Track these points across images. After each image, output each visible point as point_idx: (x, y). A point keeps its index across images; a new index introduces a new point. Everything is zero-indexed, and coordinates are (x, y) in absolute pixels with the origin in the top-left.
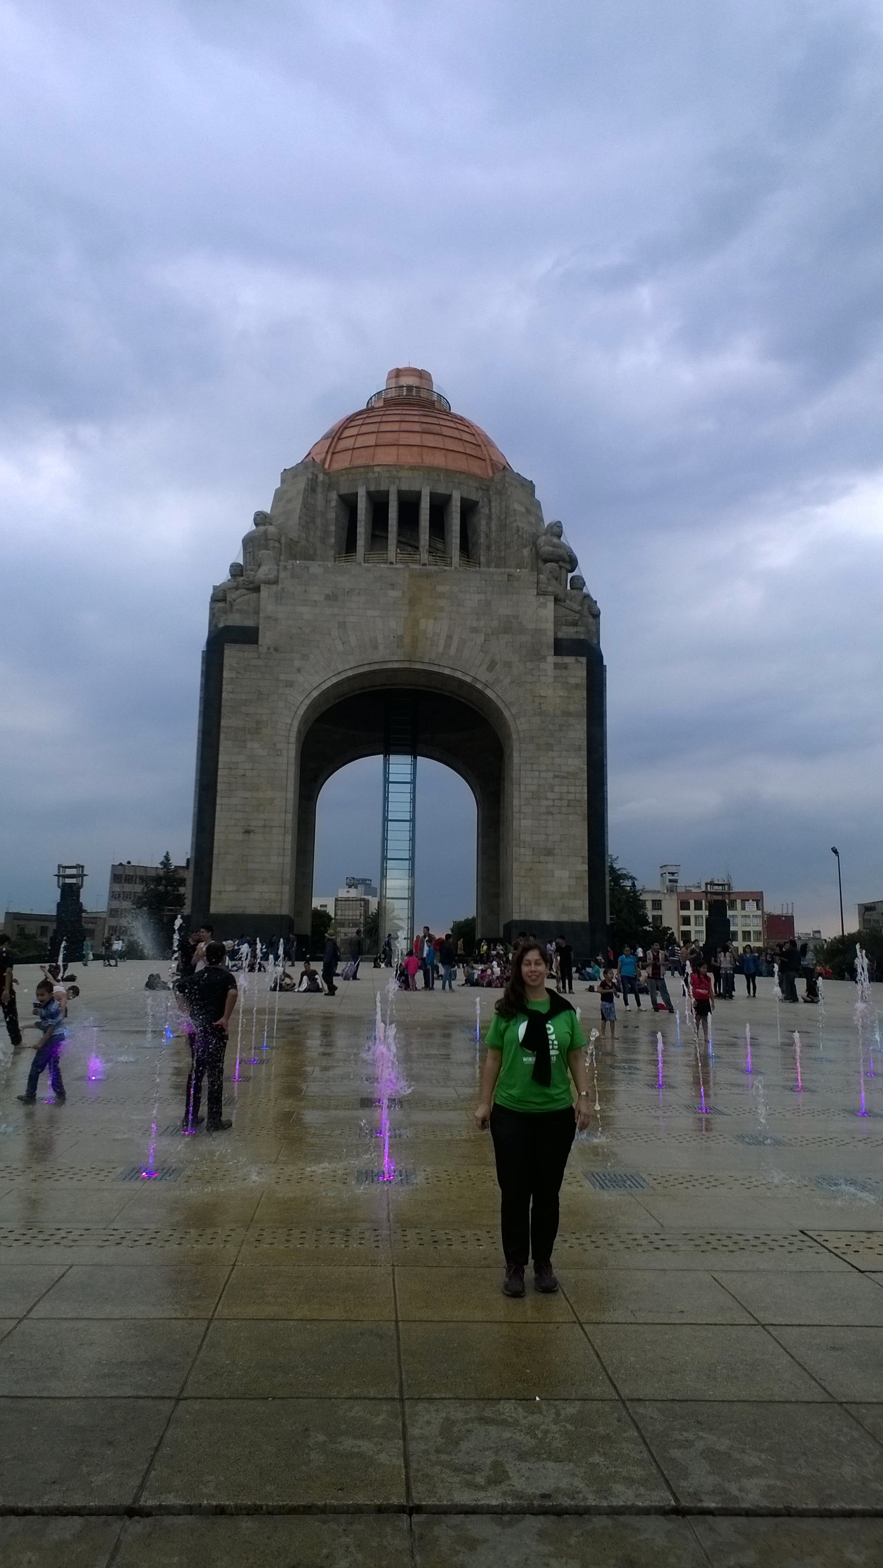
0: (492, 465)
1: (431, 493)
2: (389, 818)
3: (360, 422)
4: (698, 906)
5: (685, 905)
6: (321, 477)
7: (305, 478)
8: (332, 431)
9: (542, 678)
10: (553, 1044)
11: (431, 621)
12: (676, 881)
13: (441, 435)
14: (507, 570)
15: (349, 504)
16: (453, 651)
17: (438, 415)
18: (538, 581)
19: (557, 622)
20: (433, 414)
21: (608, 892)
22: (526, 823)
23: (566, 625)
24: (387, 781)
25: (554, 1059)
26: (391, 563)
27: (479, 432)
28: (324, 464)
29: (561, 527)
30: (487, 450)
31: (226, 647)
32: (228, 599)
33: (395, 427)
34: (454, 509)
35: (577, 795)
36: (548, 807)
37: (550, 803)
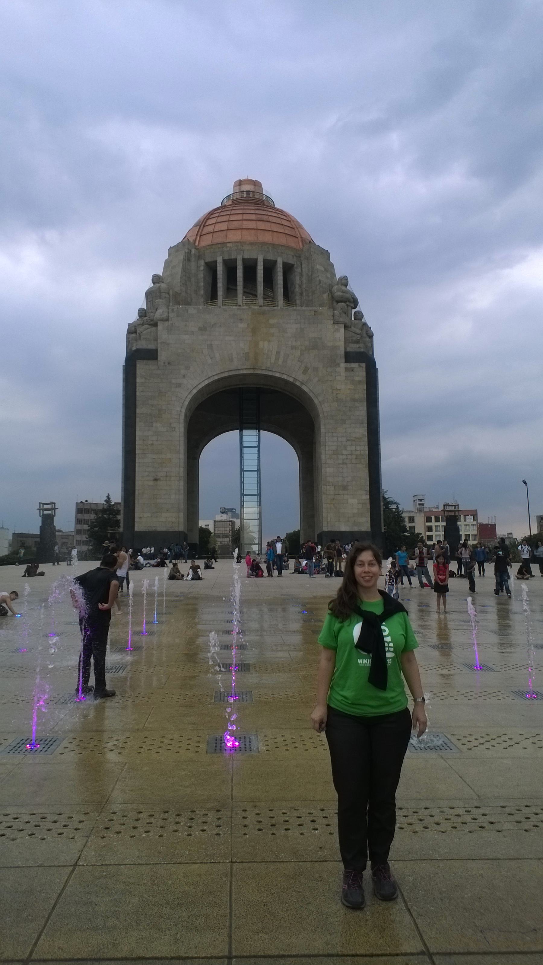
0: (302, 241)
1: (264, 260)
2: (244, 469)
3: (217, 215)
4: (437, 520)
5: (429, 520)
6: (193, 251)
7: (183, 252)
8: (199, 221)
9: (338, 378)
10: (389, 647)
11: (266, 343)
12: (423, 505)
13: (269, 222)
14: (313, 308)
15: (212, 267)
16: (280, 362)
17: (266, 209)
18: (333, 314)
19: (347, 341)
21: (382, 512)
22: (330, 470)
23: (352, 343)
24: (242, 446)
25: (389, 662)
26: (240, 306)
27: (293, 219)
28: (195, 243)
29: (347, 279)
30: (298, 231)
31: (137, 362)
32: (138, 332)
33: (240, 217)
34: (279, 269)
35: (362, 451)
36: (343, 459)
37: (345, 457)
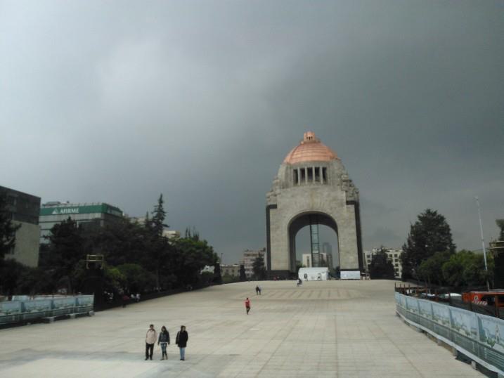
15: (296, 171)
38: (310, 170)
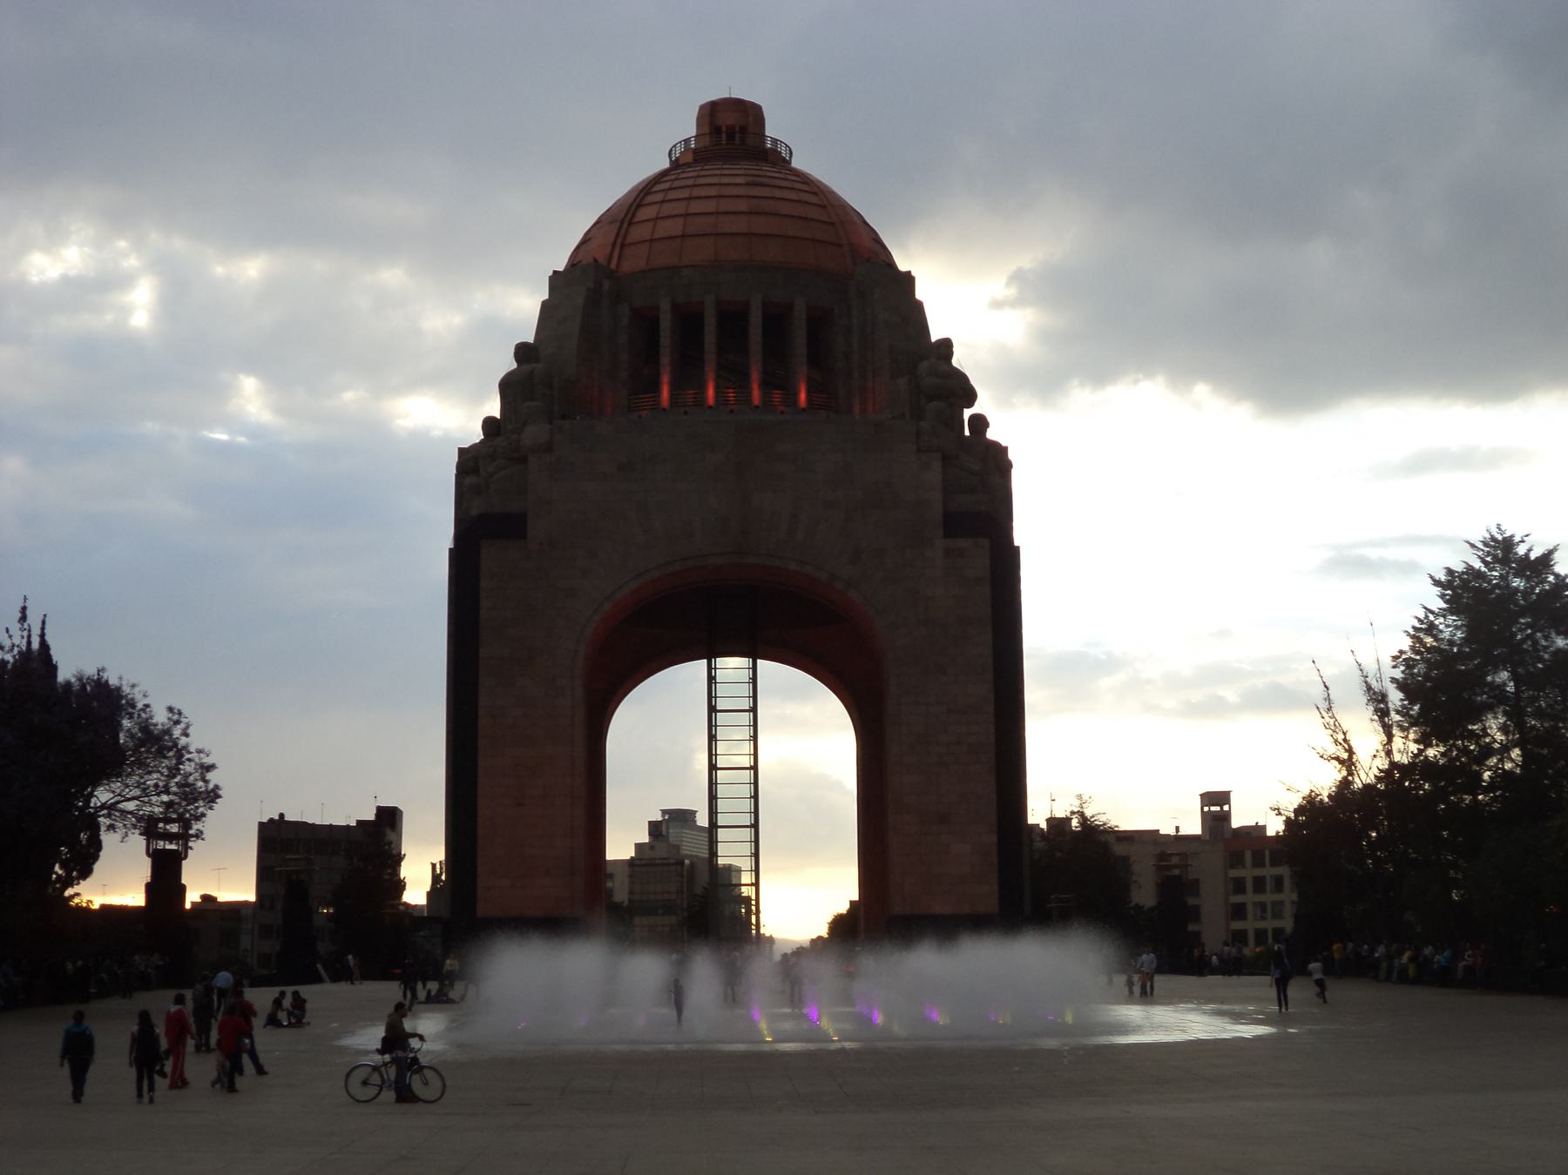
3: (659, 197)
6: (606, 284)
15: (646, 322)
20: (765, 180)
38: (733, 321)
